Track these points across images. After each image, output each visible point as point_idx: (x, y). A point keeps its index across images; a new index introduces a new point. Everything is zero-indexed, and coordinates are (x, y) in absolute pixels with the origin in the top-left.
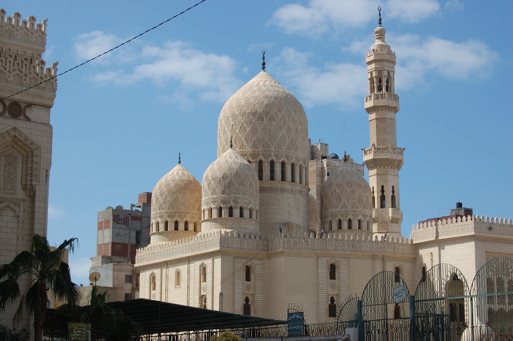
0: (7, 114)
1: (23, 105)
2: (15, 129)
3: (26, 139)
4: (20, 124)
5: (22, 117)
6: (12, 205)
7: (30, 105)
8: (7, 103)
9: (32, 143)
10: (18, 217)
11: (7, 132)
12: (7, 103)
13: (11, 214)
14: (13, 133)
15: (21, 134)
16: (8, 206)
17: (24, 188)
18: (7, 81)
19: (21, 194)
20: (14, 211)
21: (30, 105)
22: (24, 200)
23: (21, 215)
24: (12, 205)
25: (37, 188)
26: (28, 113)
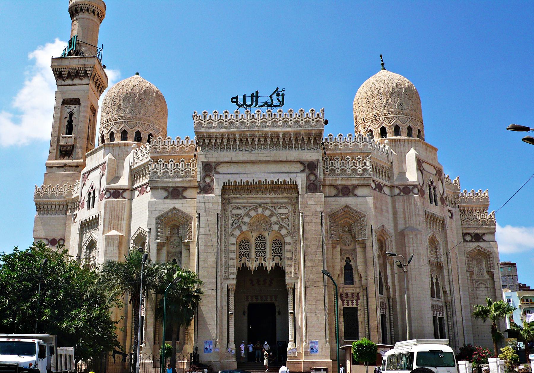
0: (474, 240)
1: (481, 235)
2: (478, 246)
3: (485, 250)
4: (481, 244)
5: (481, 240)
6: (483, 282)
7: (484, 234)
8: (473, 235)
9: (488, 251)
10: (487, 287)
11: (475, 248)
12: (473, 235)
13: (484, 286)
14: (478, 248)
15: (482, 248)
16: (482, 283)
17: (488, 273)
18: (471, 225)
19: (487, 276)
20: (485, 285)
21: (484, 234)
22: (489, 279)
23: (489, 286)
24: (483, 282)
25: (494, 273)
26: (484, 238)
